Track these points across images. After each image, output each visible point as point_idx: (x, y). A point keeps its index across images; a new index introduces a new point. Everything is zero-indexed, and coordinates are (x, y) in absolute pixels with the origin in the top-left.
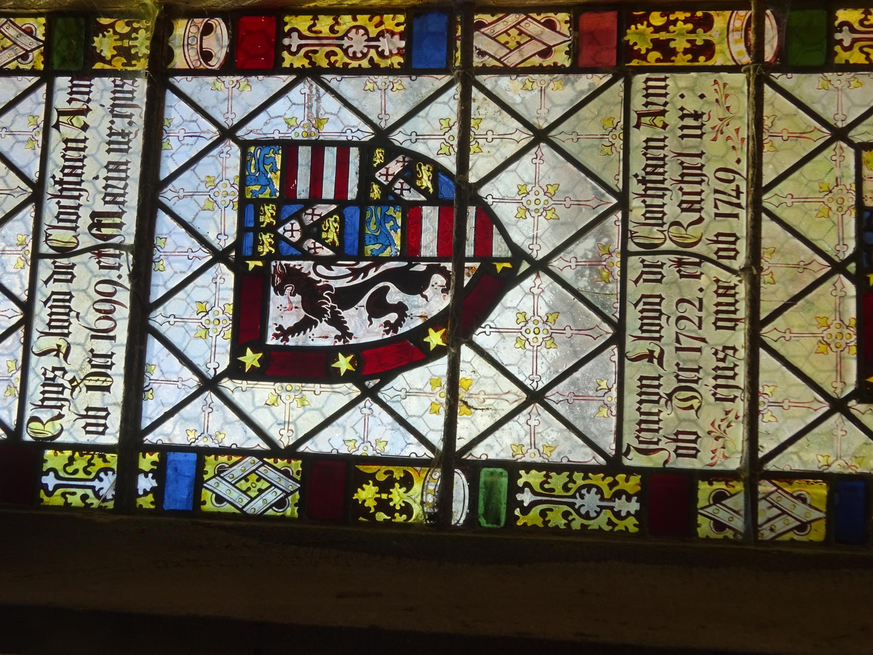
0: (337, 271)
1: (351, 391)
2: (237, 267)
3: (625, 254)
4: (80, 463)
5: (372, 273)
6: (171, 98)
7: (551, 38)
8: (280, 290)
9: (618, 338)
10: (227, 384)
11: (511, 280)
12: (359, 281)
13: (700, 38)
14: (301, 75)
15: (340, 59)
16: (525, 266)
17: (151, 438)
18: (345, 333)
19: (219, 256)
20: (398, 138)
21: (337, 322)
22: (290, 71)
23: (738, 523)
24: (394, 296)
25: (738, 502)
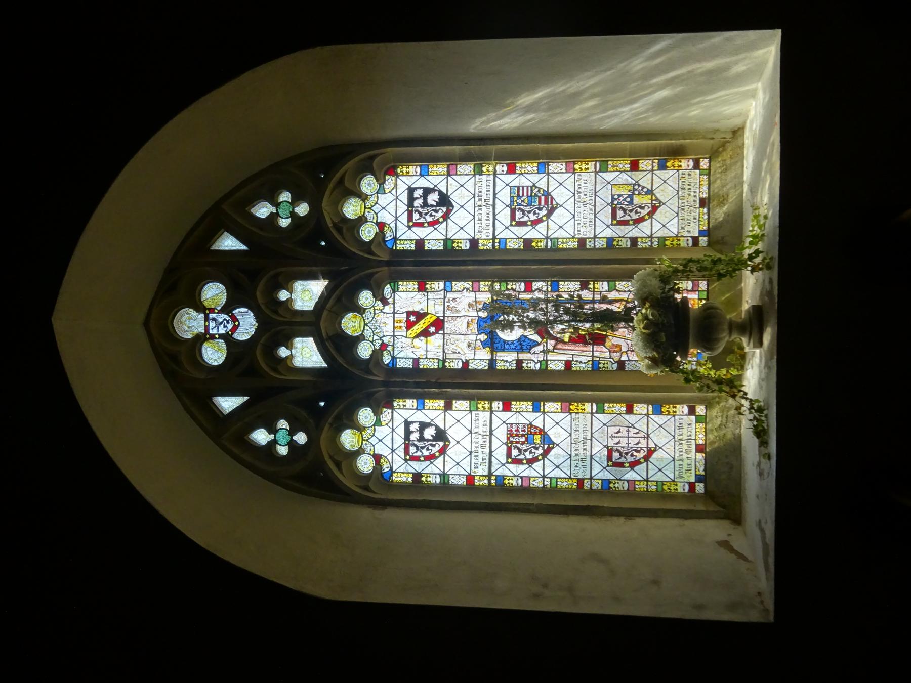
0: (524, 446)
1: (527, 466)
2: (507, 445)
3: (571, 443)
4: (481, 478)
5: (530, 447)
6: (493, 415)
7: (557, 407)
8: (514, 449)
9: (570, 457)
10: (506, 465)
11: (553, 448)
12: (528, 448)
13: (583, 407)
14: (516, 412)
15: (521, 410)
16: (555, 445)
17: (494, 474)
18: (526, 457)
19: (503, 443)
20: (533, 423)
21: (524, 454)
22: (514, 411)
23: (589, 486)
24: (533, 450)
25: (589, 483)
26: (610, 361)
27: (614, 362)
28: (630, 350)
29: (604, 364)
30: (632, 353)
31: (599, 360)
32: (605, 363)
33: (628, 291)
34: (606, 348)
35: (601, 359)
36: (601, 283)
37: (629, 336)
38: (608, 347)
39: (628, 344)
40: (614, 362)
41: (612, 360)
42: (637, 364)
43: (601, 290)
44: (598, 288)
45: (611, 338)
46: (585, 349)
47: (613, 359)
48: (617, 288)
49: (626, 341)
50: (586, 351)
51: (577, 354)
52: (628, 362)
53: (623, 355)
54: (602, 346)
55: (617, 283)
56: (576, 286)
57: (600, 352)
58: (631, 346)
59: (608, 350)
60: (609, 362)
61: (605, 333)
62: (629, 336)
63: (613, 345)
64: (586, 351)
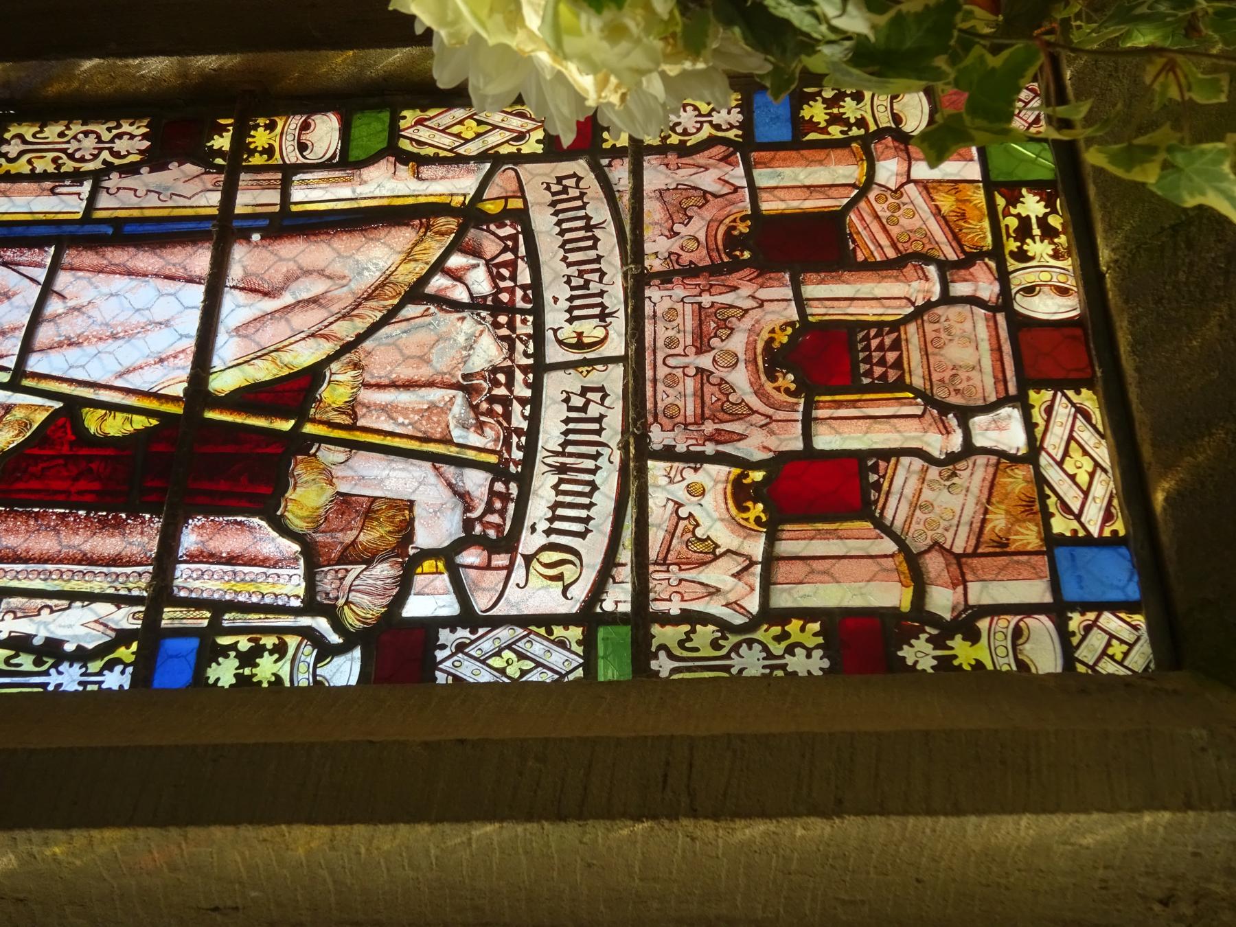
26: (309, 634)
27: (335, 639)
28: (483, 542)
29: (248, 659)
30: (501, 560)
31: (216, 627)
32: (257, 651)
33: (482, 157)
34: (283, 530)
35: (229, 619)
36: (296, 122)
37: (474, 439)
38: (298, 525)
39: (464, 497)
40: (335, 639)
41: (321, 624)
42: (537, 648)
43: (293, 157)
44: (269, 151)
45: (330, 455)
46: (109, 544)
47: (332, 613)
48: (405, 145)
49: (449, 471)
50: (116, 561)
51: (37, 584)
52: (463, 634)
53: (419, 581)
54: (256, 521)
55: (410, 116)
56: (121, 146)
57: (232, 560)
58: (489, 509)
59: (296, 548)
60: (292, 641)
61: (287, 426)
62: (474, 439)
63: (344, 501)
64: (116, 561)
